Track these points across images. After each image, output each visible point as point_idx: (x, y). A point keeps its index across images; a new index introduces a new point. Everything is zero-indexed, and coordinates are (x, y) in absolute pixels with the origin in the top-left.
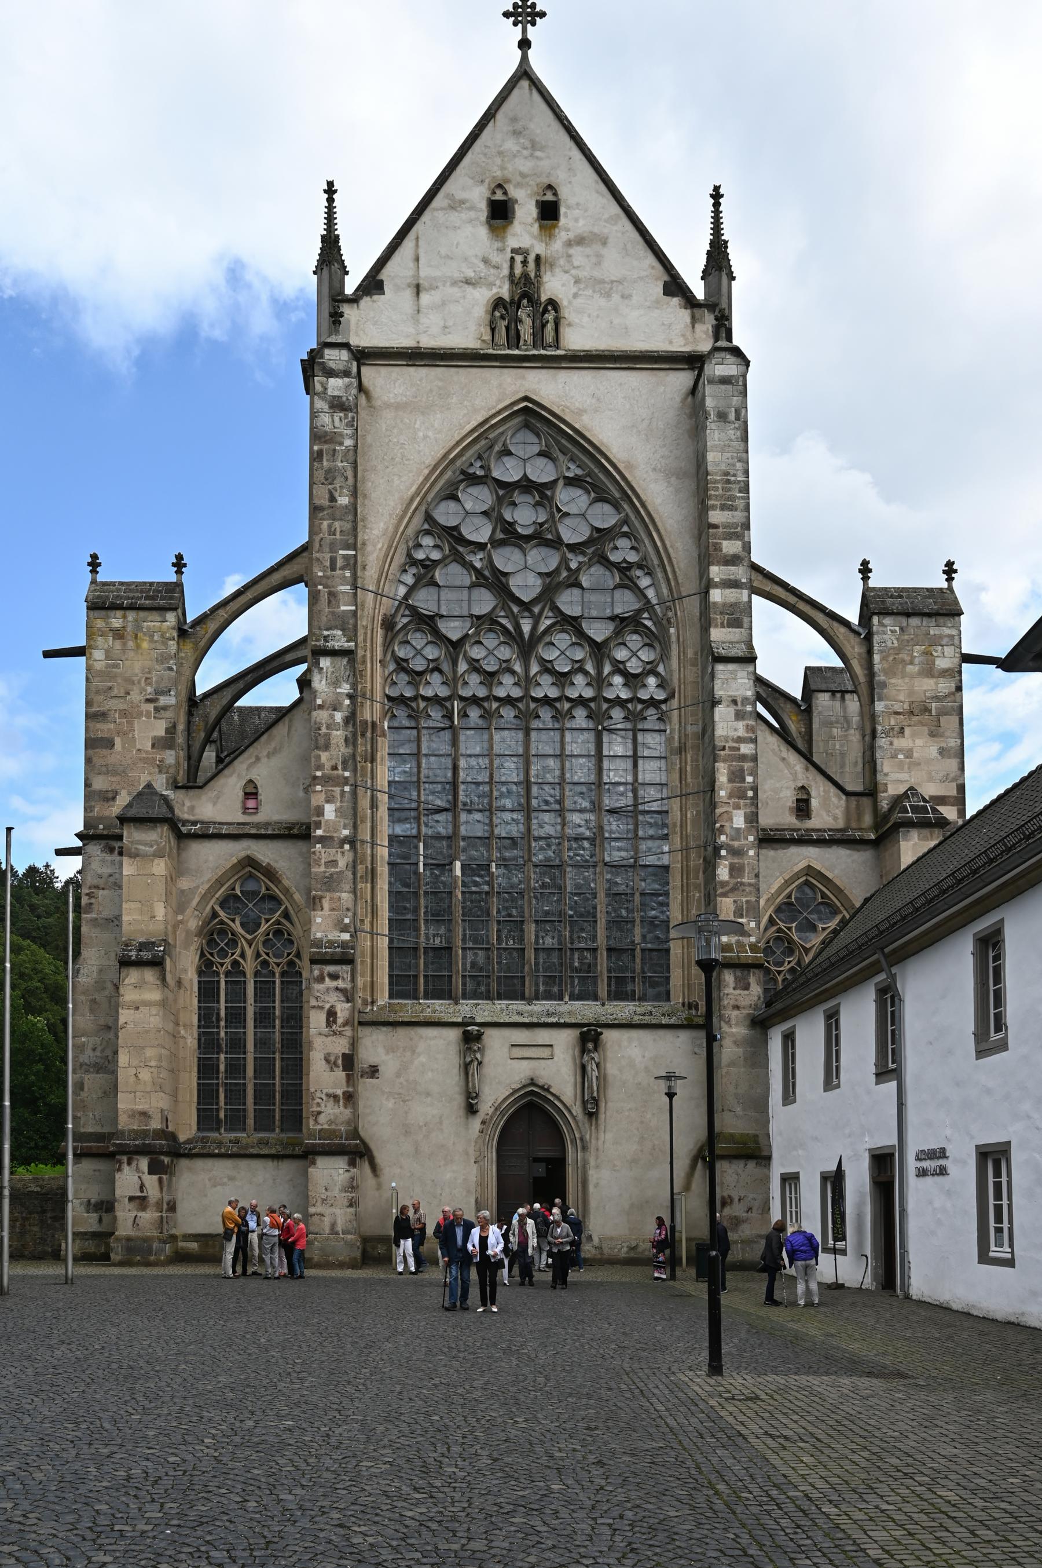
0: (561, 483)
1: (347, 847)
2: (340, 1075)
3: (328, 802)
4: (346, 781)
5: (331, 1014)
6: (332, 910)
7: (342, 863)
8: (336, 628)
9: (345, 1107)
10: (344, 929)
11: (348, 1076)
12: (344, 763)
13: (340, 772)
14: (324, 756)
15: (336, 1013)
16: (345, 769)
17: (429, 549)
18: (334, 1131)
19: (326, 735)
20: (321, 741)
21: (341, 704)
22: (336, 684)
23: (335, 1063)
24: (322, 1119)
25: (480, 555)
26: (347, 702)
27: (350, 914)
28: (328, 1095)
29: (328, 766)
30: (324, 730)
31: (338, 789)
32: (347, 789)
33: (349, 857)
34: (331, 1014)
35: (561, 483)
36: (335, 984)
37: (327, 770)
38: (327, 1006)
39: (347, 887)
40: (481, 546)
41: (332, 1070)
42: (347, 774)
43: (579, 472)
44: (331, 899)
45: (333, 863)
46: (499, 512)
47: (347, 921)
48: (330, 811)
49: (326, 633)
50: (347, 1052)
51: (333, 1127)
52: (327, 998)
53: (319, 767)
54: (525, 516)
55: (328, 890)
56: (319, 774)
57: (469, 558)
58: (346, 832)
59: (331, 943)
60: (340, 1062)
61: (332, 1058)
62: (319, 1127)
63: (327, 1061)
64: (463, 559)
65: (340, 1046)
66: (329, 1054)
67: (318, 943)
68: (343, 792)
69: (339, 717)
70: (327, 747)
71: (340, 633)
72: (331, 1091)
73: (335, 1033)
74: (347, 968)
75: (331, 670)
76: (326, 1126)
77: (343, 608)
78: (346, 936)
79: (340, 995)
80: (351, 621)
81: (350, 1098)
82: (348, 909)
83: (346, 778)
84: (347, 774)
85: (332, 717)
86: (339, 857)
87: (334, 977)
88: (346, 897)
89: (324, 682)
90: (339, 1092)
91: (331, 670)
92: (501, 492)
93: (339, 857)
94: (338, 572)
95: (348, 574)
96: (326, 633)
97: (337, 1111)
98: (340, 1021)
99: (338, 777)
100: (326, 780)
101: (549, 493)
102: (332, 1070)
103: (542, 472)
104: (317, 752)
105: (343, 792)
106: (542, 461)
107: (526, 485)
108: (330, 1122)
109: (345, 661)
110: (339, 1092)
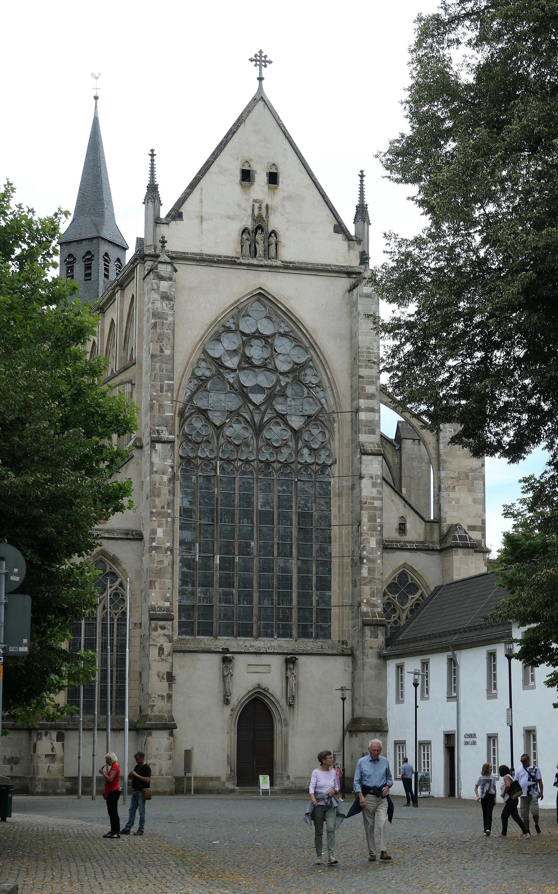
0: (277, 335)
1: (169, 553)
2: (165, 684)
3: (159, 527)
4: (169, 515)
5: (161, 649)
6: (160, 589)
7: (167, 562)
8: (163, 425)
9: (168, 702)
10: (167, 600)
11: (169, 684)
12: (168, 505)
13: (166, 510)
14: (157, 500)
15: (163, 649)
16: (168, 508)
17: (204, 371)
18: (162, 716)
19: (158, 488)
20: (156, 492)
21: (167, 471)
22: (164, 459)
23: (163, 678)
24: (155, 709)
25: (232, 375)
26: (170, 470)
27: (170, 591)
28: (159, 696)
29: (159, 506)
30: (157, 486)
31: (164, 520)
32: (169, 519)
33: (170, 558)
34: (161, 649)
35: (277, 335)
36: (163, 632)
37: (159, 509)
38: (159, 645)
39: (169, 575)
40: (234, 371)
41: (161, 681)
42: (169, 511)
43: (287, 329)
44: (160, 583)
45: (161, 562)
46: (244, 351)
47: (168, 595)
48: (160, 532)
49: (157, 428)
50: (169, 671)
51: (161, 714)
52: (159, 640)
53: (154, 507)
54: (256, 352)
55: (159, 578)
56: (154, 510)
57: (227, 376)
58: (168, 545)
59: (160, 608)
60: (165, 677)
61: (161, 675)
62: (153, 714)
63: (159, 676)
64: (224, 377)
65: (164, 668)
66: (159, 672)
67: (153, 608)
68: (167, 521)
69: (165, 478)
70: (159, 496)
71: (165, 428)
72: (160, 693)
73: (163, 660)
74: (170, 623)
75: (162, 451)
76: (157, 714)
77: (166, 414)
78: (168, 604)
79: (166, 638)
80: (171, 422)
81: (170, 697)
82: (169, 589)
83: (169, 513)
84: (169, 511)
85: (162, 478)
86: (164, 558)
87: (163, 628)
88: (168, 582)
89: (158, 458)
90: (165, 694)
91: (162, 451)
92: (244, 338)
93: (164, 558)
94: (164, 393)
95: (169, 394)
96: (157, 428)
97: (163, 704)
98: (166, 653)
99: (165, 512)
100: (159, 514)
101: (270, 340)
102: (161, 681)
103: (267, 328)
104: (153, 498)
105: (167, 521)
106: (265, 322)
107: (257, 335)
108: (160, 711)
109: (169, 446)
110: (165, 694)
